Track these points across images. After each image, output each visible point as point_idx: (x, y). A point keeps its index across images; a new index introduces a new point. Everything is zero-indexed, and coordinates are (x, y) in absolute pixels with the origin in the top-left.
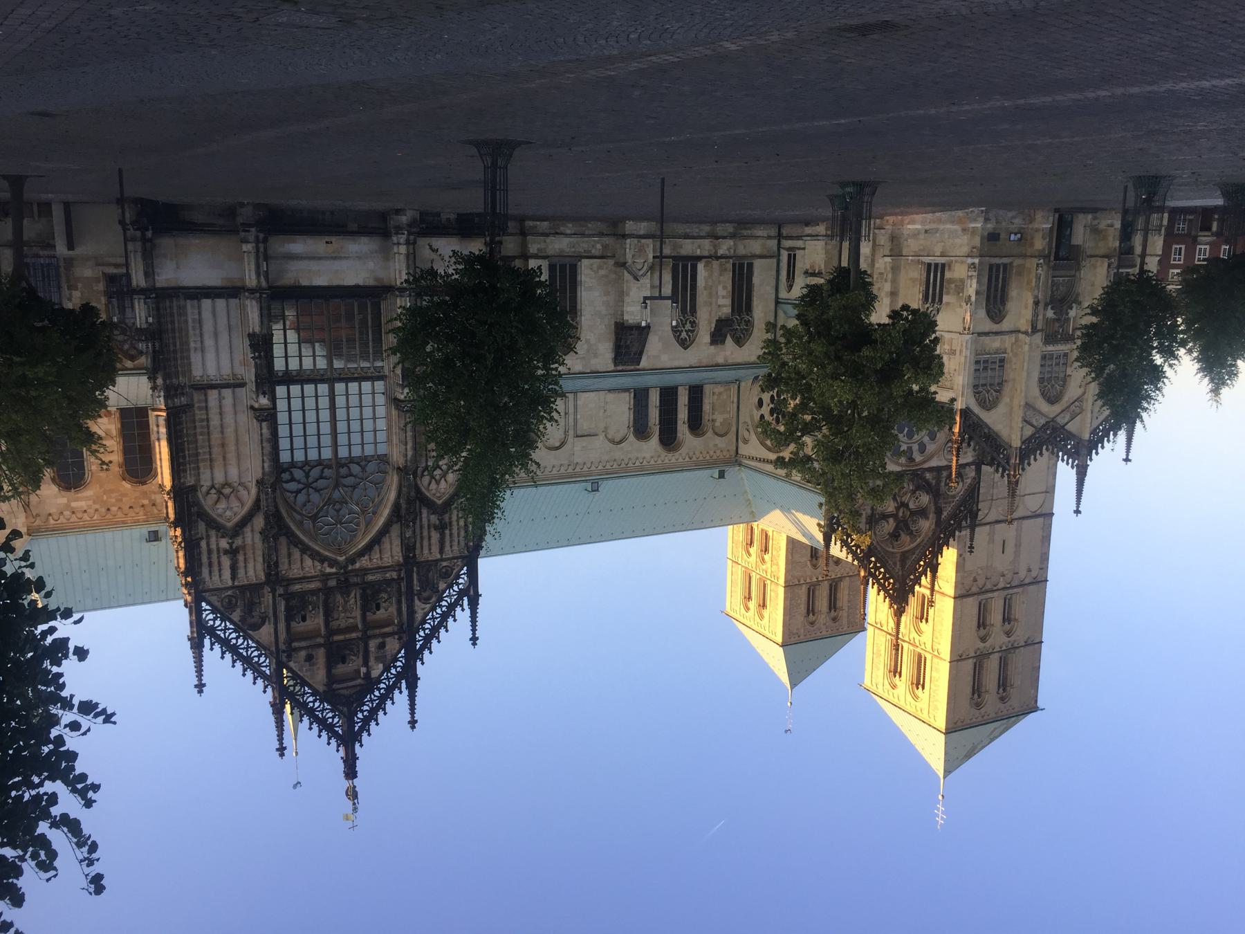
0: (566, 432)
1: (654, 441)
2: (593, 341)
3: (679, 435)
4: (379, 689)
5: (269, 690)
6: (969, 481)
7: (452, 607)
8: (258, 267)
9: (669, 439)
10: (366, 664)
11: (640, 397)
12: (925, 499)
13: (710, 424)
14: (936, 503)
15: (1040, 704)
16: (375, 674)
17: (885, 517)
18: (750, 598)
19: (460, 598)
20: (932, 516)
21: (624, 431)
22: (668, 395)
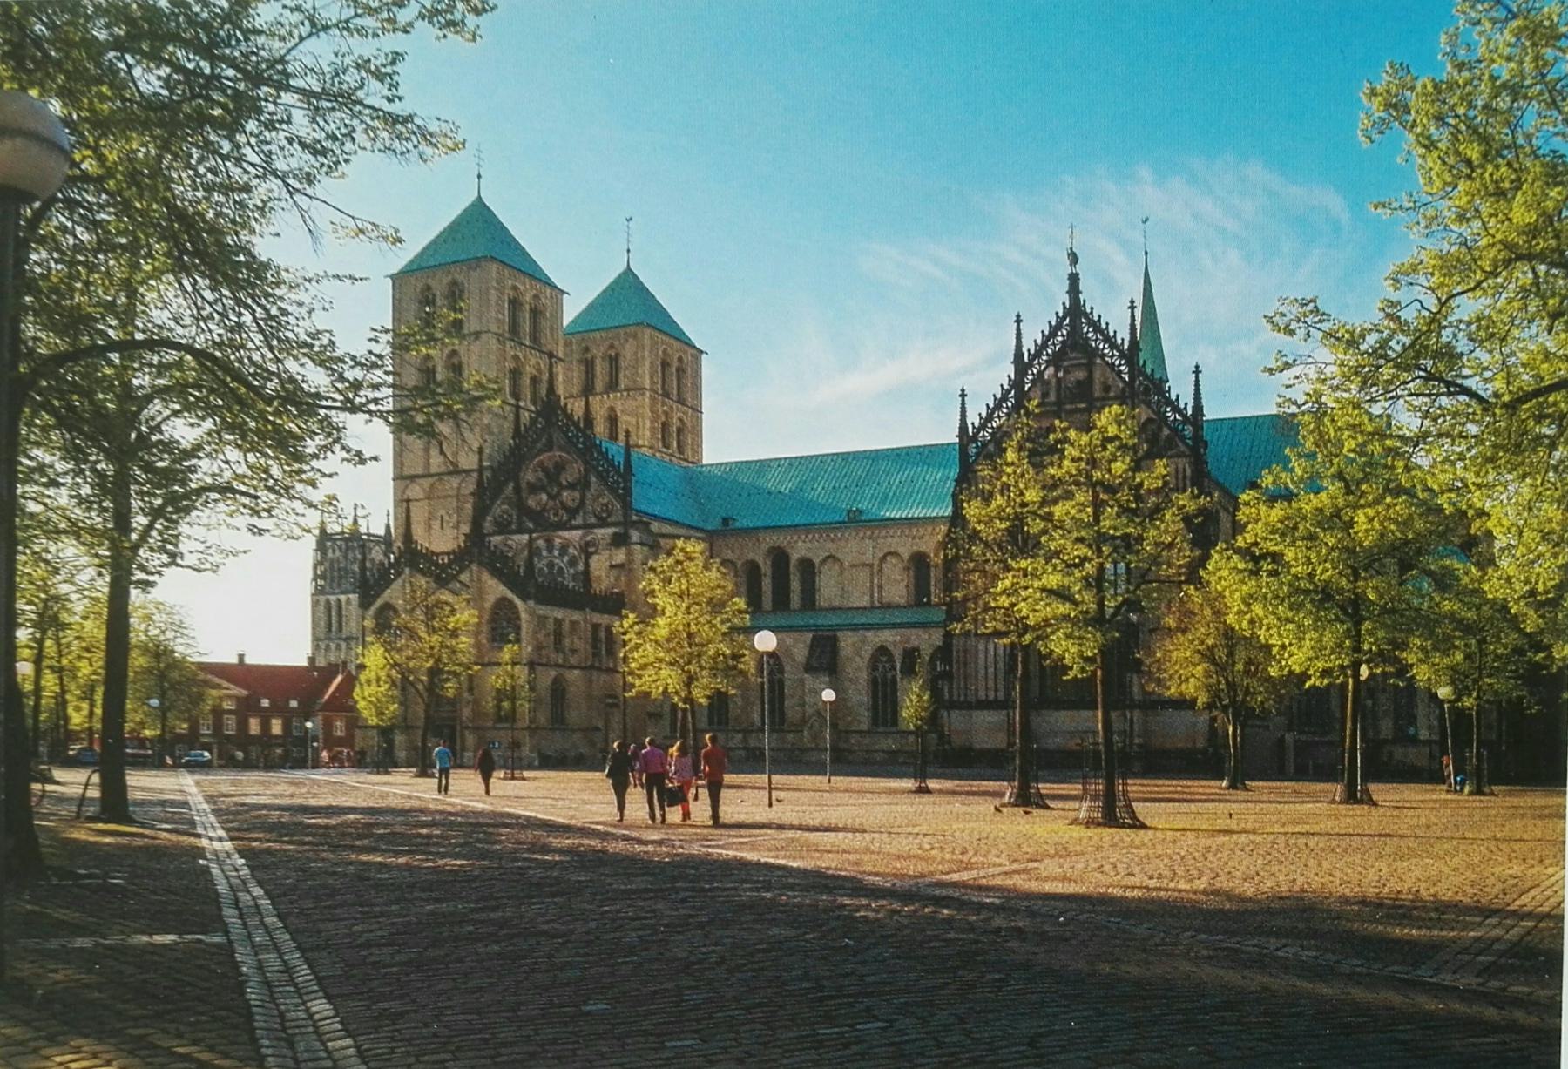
0: (881, 570)
1: (795, 556)
2: (857, 659)
3: (769, 562)
4: (1048, 355)
5: (1141, 363)
6: (489, 518)
7: (983, 427)
8: (1131, 727)
9: (780, 558)
10: (1059, 380)
11: (809, 601)
12: (531, 502)
13: (741, 573)
14: (520, 498)
15: (390, 282)
16: (1051, 370)
17: (572, 486)
18: (678, 370)
19: (976, 434)
20: (524, 485)
21: (825, 569)
22: (781, 602)
